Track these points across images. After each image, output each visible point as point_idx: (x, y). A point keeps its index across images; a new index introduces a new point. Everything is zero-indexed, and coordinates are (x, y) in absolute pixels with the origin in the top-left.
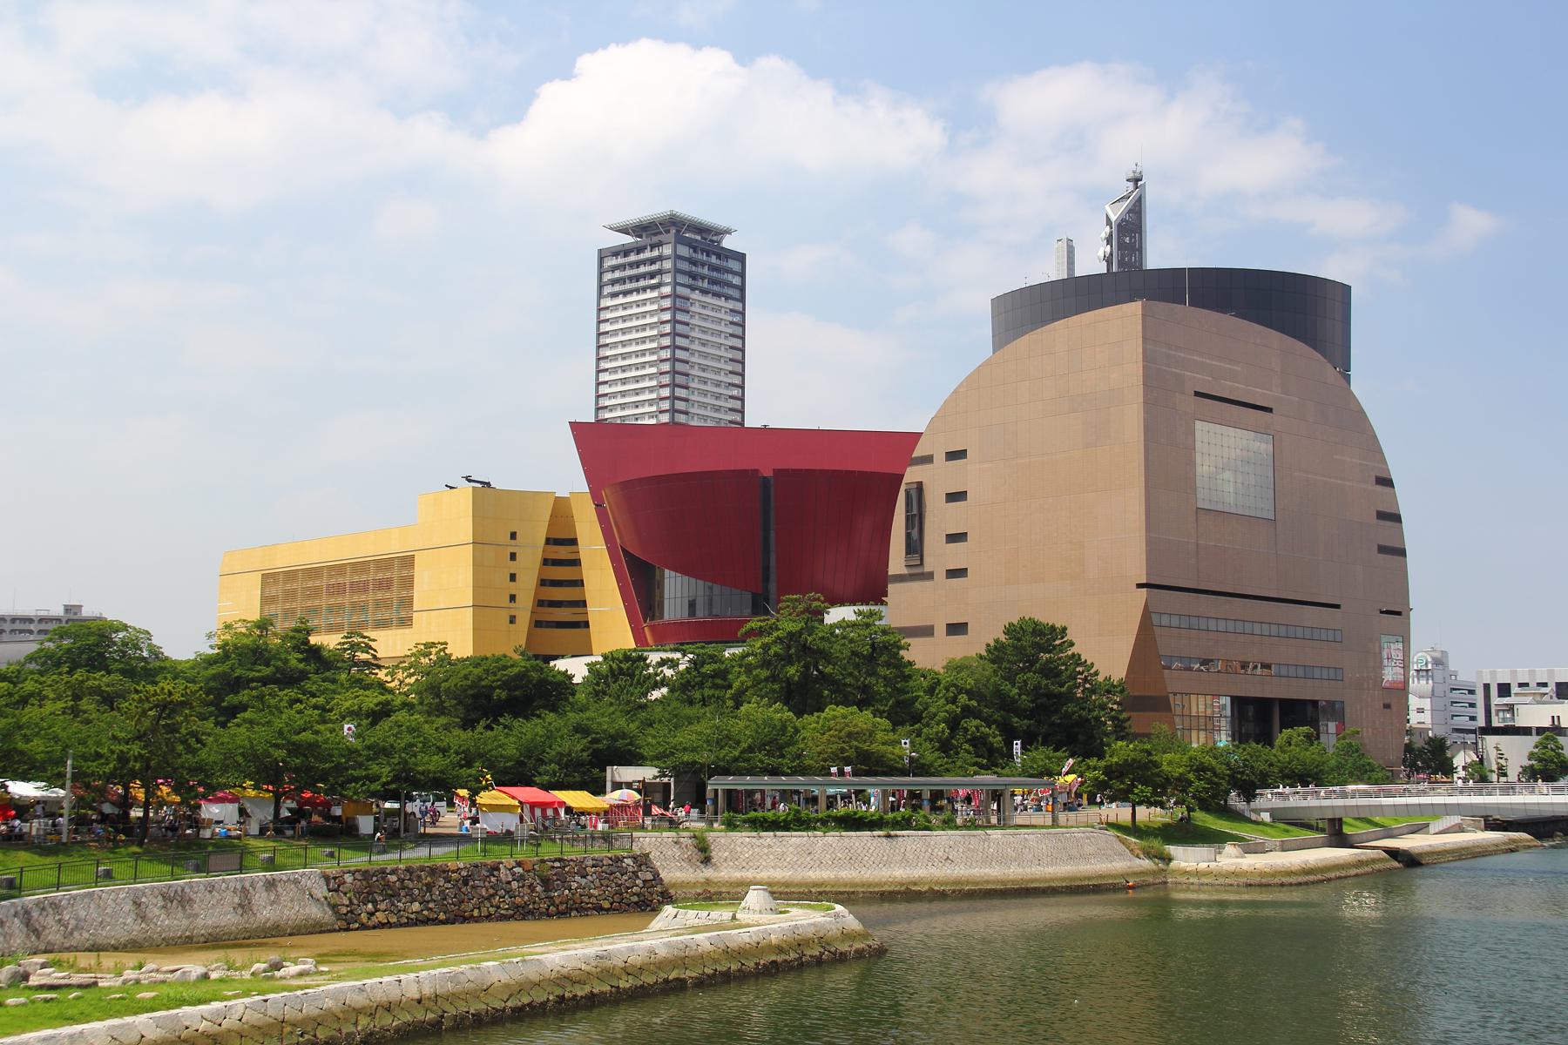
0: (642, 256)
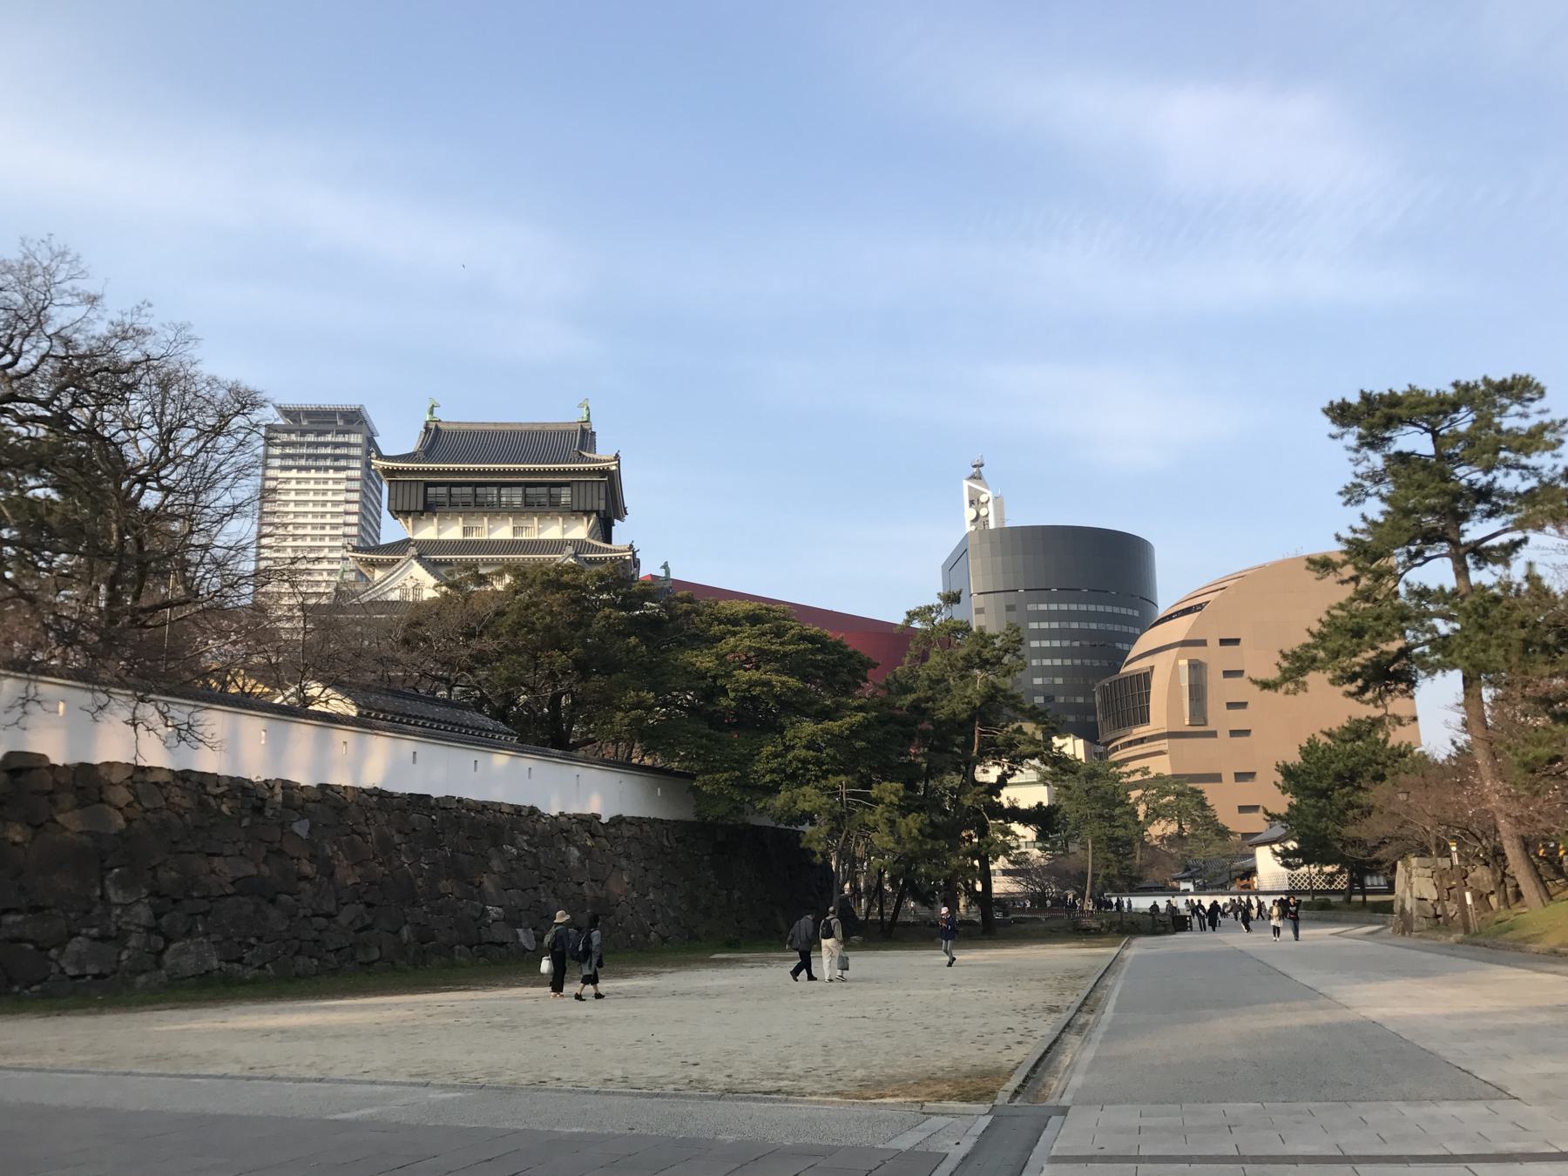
0: (321, 439)
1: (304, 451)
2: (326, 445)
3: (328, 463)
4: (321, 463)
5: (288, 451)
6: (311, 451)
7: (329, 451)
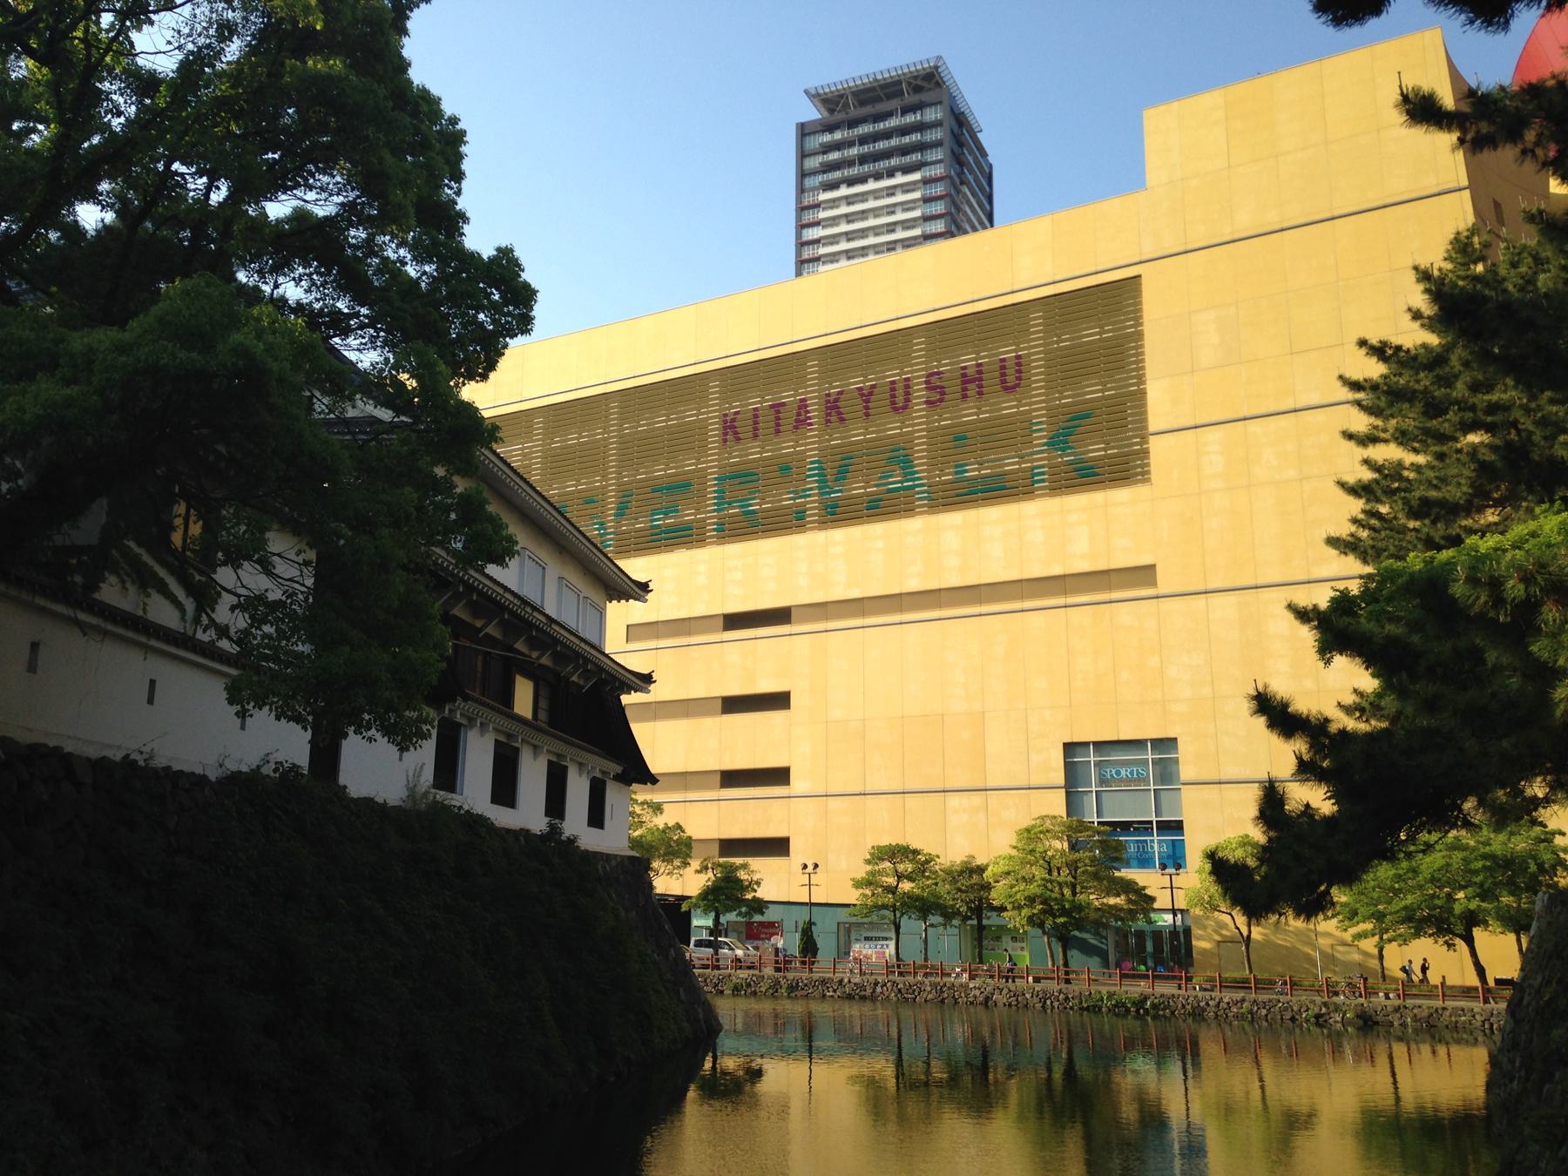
1: (854, 151)
2: (887, 135)
3: (894, 162)
4: (883, 165)
5: (834, 156)
6: (866, 149)
7: (894, 142)
